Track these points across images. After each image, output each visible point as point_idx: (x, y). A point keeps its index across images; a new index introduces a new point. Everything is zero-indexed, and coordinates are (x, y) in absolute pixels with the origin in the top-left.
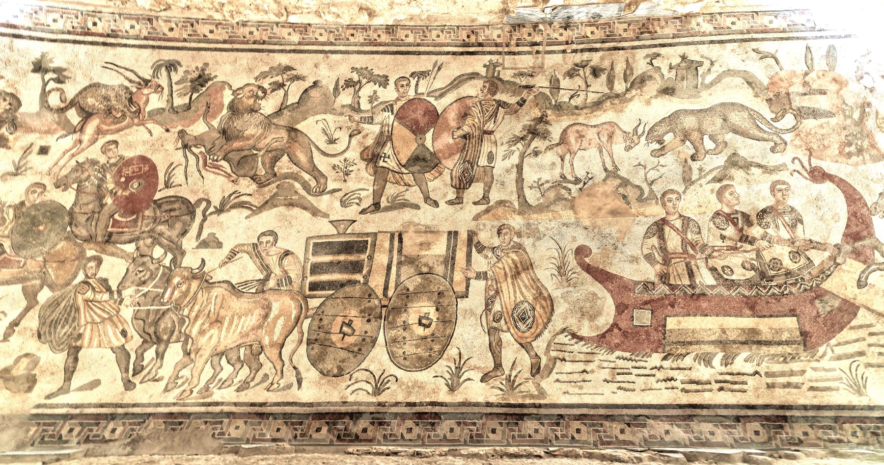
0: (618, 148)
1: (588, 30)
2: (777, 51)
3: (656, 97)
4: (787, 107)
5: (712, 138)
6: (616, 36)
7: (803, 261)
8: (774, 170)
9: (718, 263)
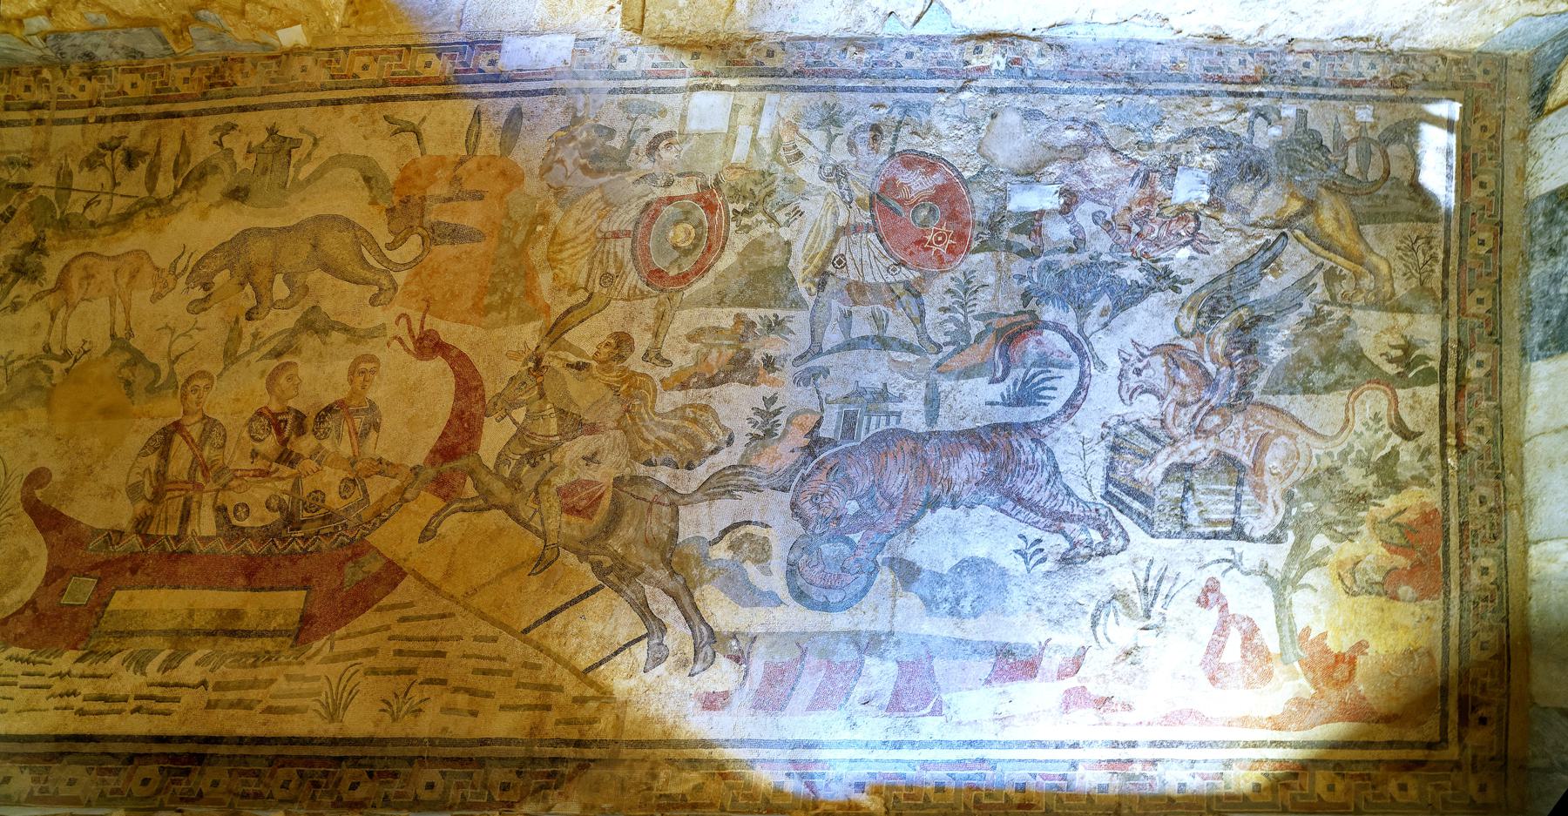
0: (140, 298)
1: (127, 80)
2: (424, 119)
3: (219, 205)
4: (416, 223)
5: (288, 281)
6: (170, 90)
7: (357, 495)
8: (363, 337)
9: (231, 499)
